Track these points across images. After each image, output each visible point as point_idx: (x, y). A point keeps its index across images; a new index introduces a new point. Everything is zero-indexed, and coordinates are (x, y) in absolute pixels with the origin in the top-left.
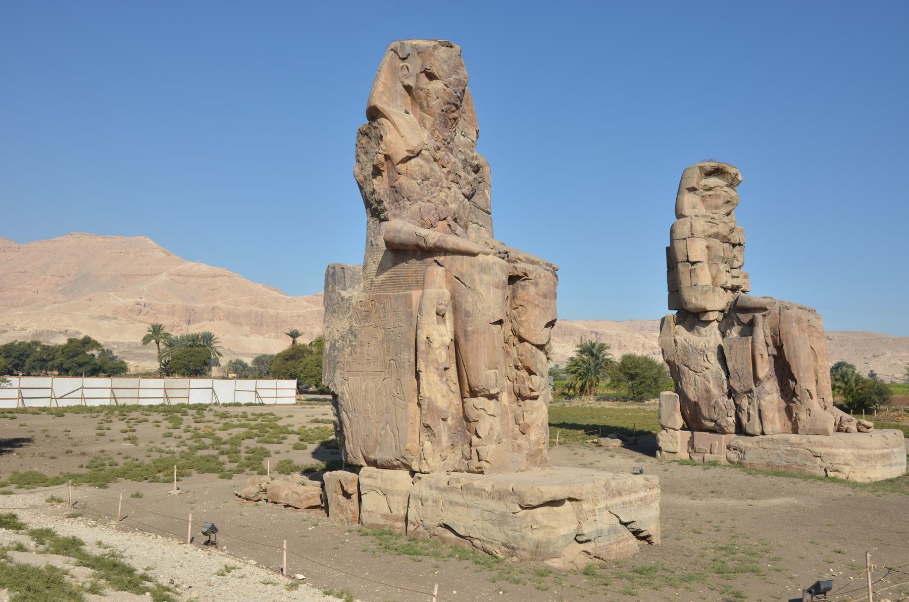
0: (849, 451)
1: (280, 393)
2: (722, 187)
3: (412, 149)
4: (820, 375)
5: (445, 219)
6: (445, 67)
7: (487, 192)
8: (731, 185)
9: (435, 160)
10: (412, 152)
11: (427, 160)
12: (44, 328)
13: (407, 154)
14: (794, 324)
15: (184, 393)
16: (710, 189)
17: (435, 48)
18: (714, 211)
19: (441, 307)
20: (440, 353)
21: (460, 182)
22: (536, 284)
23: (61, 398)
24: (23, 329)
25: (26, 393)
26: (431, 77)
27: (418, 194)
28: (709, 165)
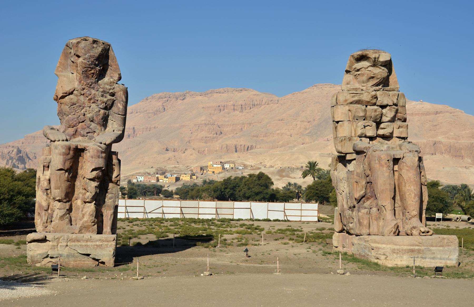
0: (389, 246)
1: (304, 213)
2: (366, 68)
4: (407, 196)
6: (83, 51)
7: (119, 105)
8: (374, 65)
10: (66, 93)
11: (76, 96)
12: (286, 165)
13: (62, 95)
14: (377, 162)
15: (230, 211)
16: (358, 70)
17: (78, 43)
18: (363, 85)
19: (45, 164)
20: (44, 183)
22: (89, 152)
23: (150, 213)
24: (272, 167)
25: (129, 209)
26: (79, 57)
27: (68, 112)
28: (358, 53)
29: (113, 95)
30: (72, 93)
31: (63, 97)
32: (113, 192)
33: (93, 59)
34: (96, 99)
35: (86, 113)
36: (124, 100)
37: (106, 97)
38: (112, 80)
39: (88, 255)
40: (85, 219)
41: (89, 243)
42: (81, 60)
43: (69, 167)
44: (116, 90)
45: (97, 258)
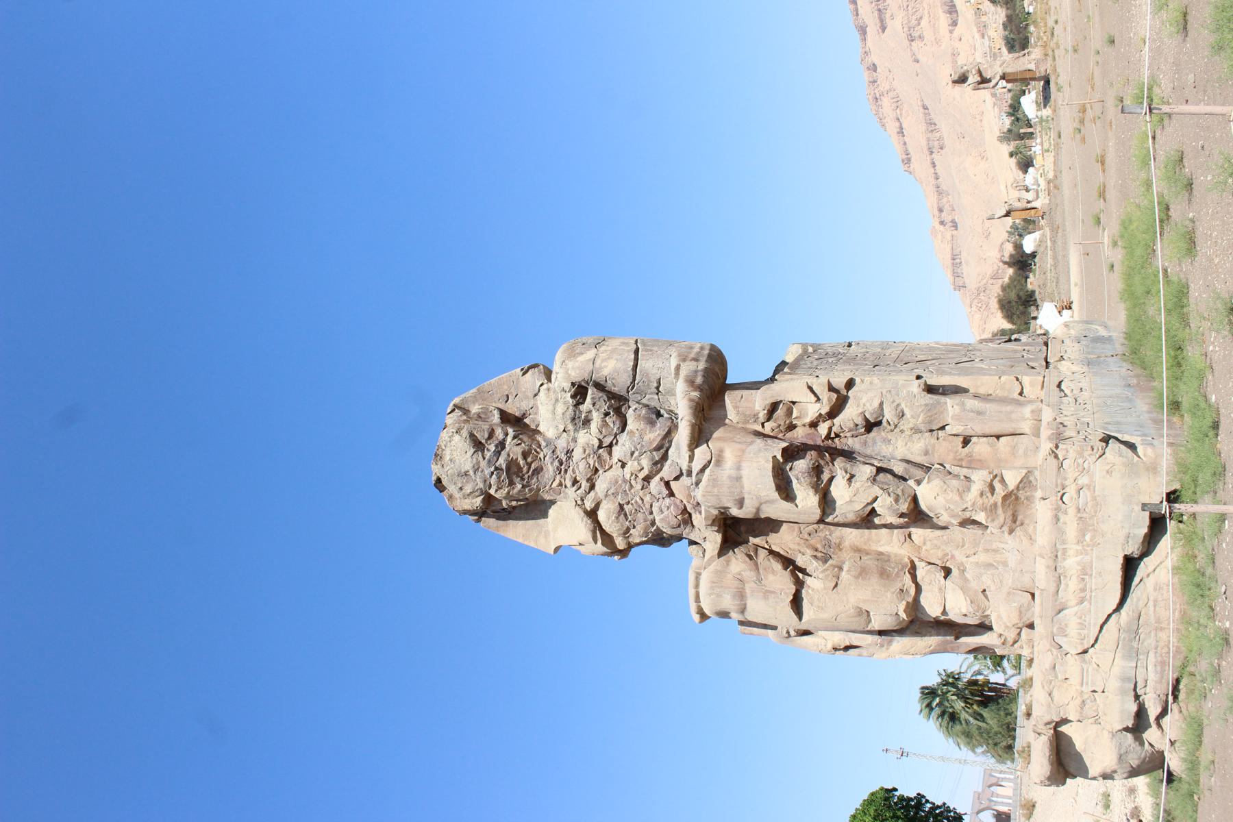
3: (590, 535)
5: (667, 484)
7: (605, 372)
9: (592, 487)
13: (599, 542)
21: (607, 442)
29: (580, 392)
30: (592, 514)
31: (607, 539)
32: (876, 404)
33: (483, 464)
34: (596, 443)
35: (642, 475)
36: (591, 354)
37: (590, 412)
38: (542, 394)
39: (1130, 565)
40: (981, 517)
41: (1071, 563)
42: (492, 492)
43: (786, 575)
44: (567, 386)
45: (1145, 530)
